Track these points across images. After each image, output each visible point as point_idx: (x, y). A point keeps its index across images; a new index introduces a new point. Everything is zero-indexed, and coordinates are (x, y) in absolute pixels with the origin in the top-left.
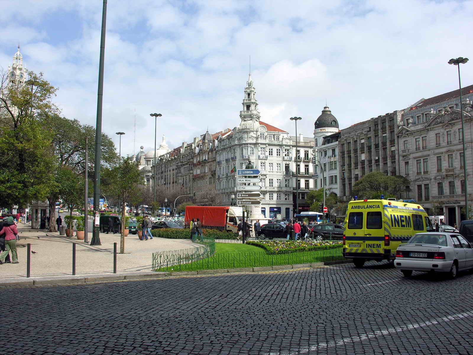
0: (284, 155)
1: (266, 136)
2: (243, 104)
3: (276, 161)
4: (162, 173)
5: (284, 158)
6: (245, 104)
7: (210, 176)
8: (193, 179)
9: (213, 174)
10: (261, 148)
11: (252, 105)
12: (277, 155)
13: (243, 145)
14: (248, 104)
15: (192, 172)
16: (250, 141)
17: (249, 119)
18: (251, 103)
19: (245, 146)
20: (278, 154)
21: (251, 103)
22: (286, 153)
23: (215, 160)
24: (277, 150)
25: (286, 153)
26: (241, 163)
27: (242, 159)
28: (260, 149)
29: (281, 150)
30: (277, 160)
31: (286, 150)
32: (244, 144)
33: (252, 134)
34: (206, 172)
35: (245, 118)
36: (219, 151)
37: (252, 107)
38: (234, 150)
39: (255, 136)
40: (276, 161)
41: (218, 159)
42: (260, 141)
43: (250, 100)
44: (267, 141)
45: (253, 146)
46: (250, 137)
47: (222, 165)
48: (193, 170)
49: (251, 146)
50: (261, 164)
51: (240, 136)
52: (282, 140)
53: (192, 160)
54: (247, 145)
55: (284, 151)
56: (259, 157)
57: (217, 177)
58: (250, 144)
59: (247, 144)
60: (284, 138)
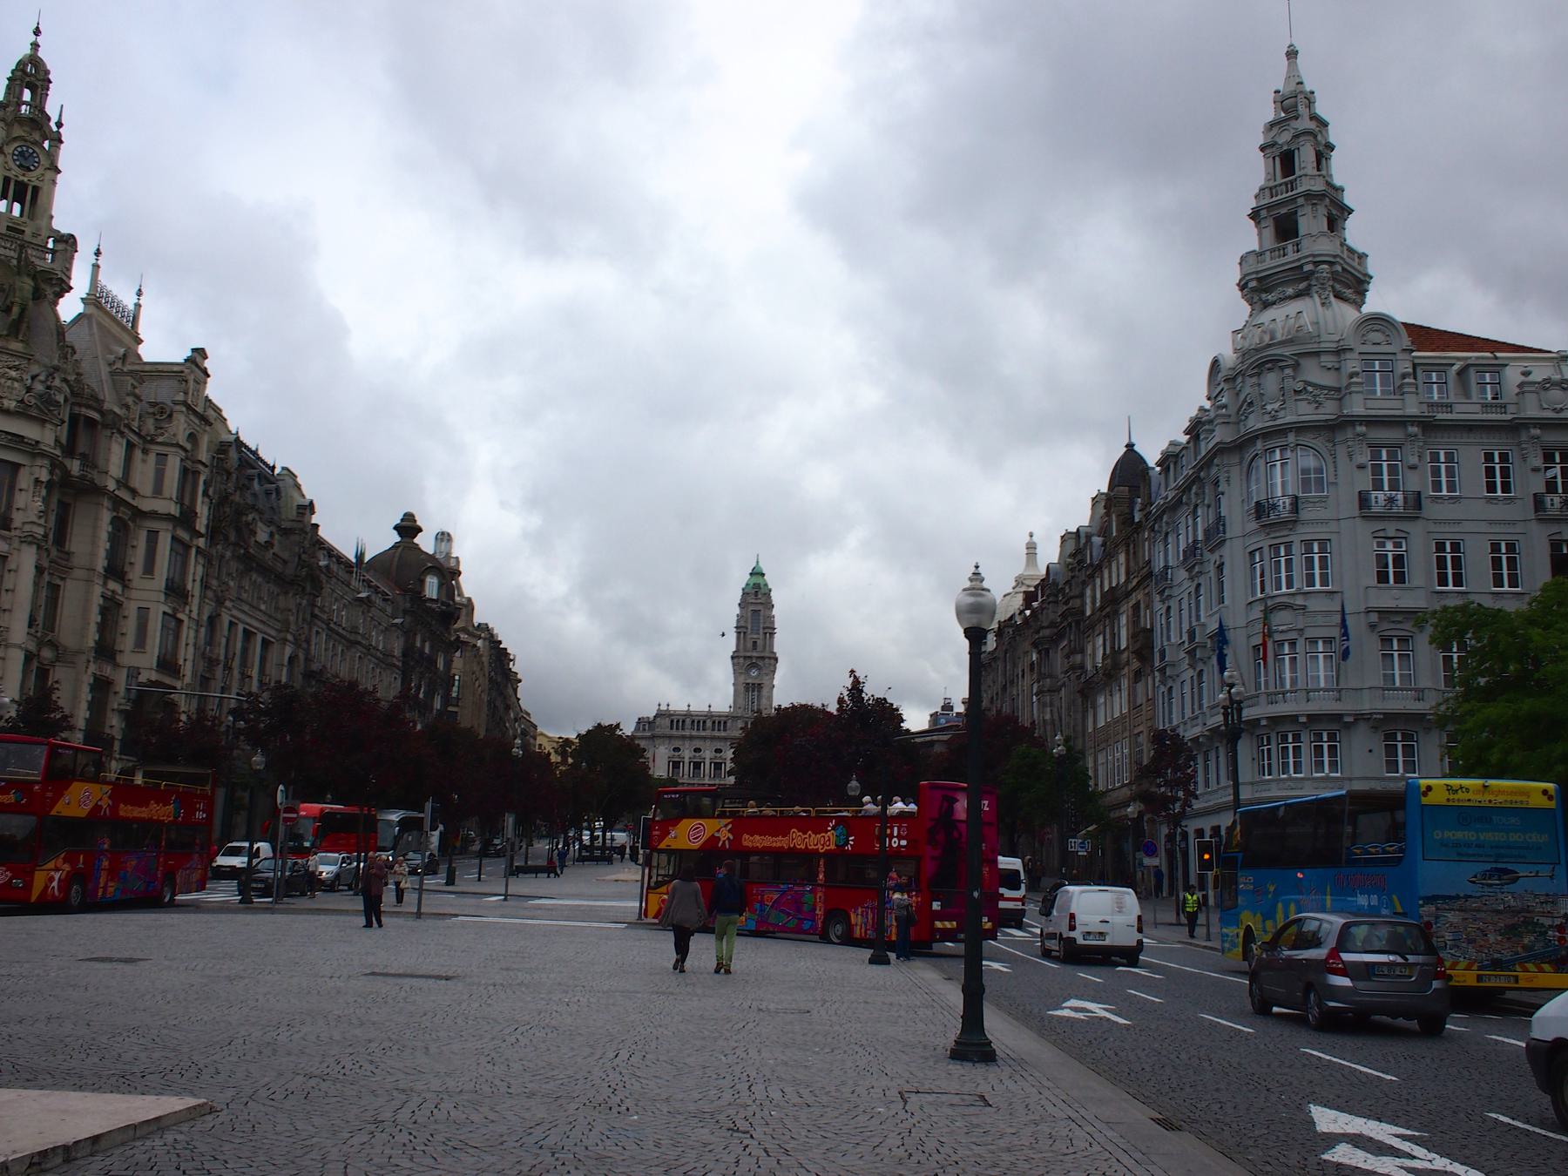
0: (1542, 489)
1: (1404, 376)
2: (1255, 215)
3: (1483, 527)
4: (1004, 688)
5: (1538, 502)
6: (1264, 213)
7: (1136, 665)
8: (1081, 692)
9: (1144, 642)
10: (1375, 448)
11: (1308, 209)
12: (1491, 488)
13: (1259, 445)
14: (1283, 211)
15: (1078, 658)
16: (1303, 411)
17: (1290, 291)
18: (1301, 201)
19: (1270, 444)
20: (1498, 479)
21: (1301, 201)
22: (1550, 474)
23: (1150, 574)
24: (1489, 457)
25: (1550, 474)
26: (1252, 553)
27: (1253, 525)
28: (1364, 457)
29: (1514, 456)
30: (1491, 522)
31: (1548, 458)
32: (1266, 434)
33: (1314, 373)
34: (1123, 646)
35: (1268, 290)
36: (1160, 517)
37: (1310, 222)
38: (1217, 484)
39: (1327, 380)
40: (1483, 527)
41: (1159, 564)
42: (1356, 407)
43: (1292, 186)
44: (1412, 408)
45: (1319, 442)
46: (1299, 386)
47: (1175, 591)
48: (1082, 651)
49: (1307, 439)
50: (1382, 545)
51: (1242, 397)
52: (1521, 393)
53: (1078, 602)
54: (1280, 441)
55: (1538, 462)
56: (1364, 500)
57: (1157, 656)
58: (1301, 428)
59: (1282, 431)
60: (1531, 378)
